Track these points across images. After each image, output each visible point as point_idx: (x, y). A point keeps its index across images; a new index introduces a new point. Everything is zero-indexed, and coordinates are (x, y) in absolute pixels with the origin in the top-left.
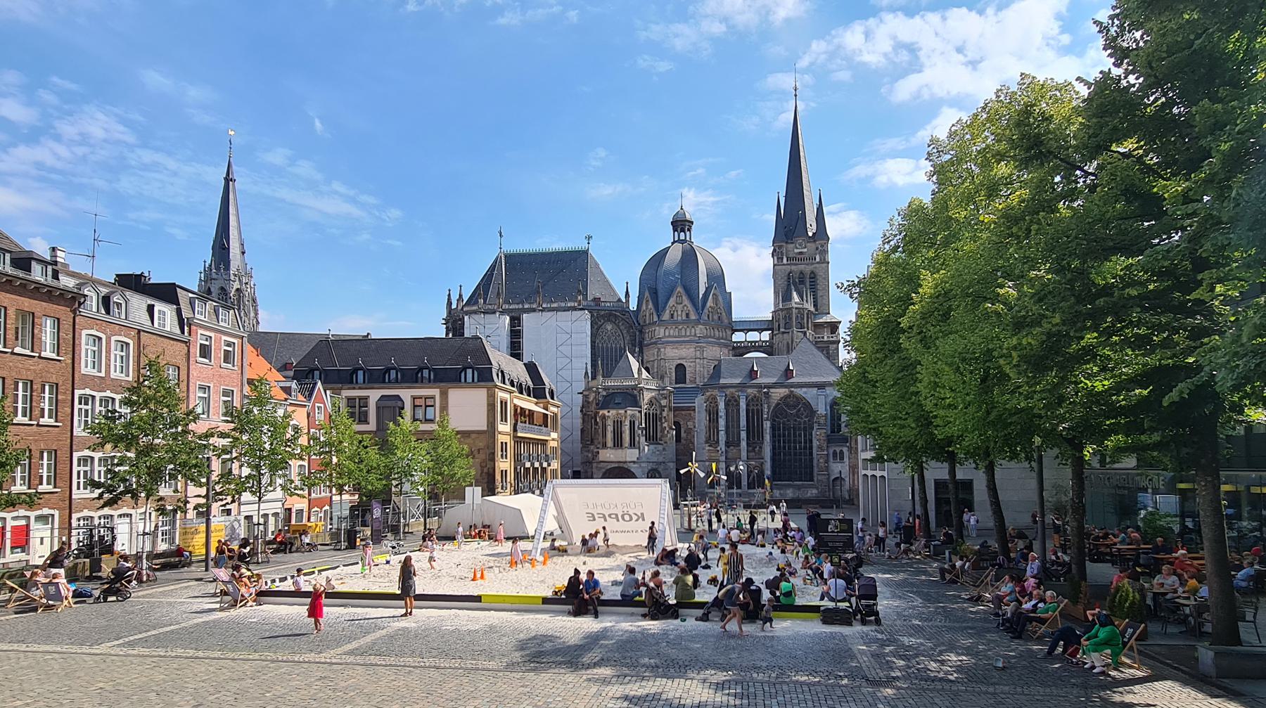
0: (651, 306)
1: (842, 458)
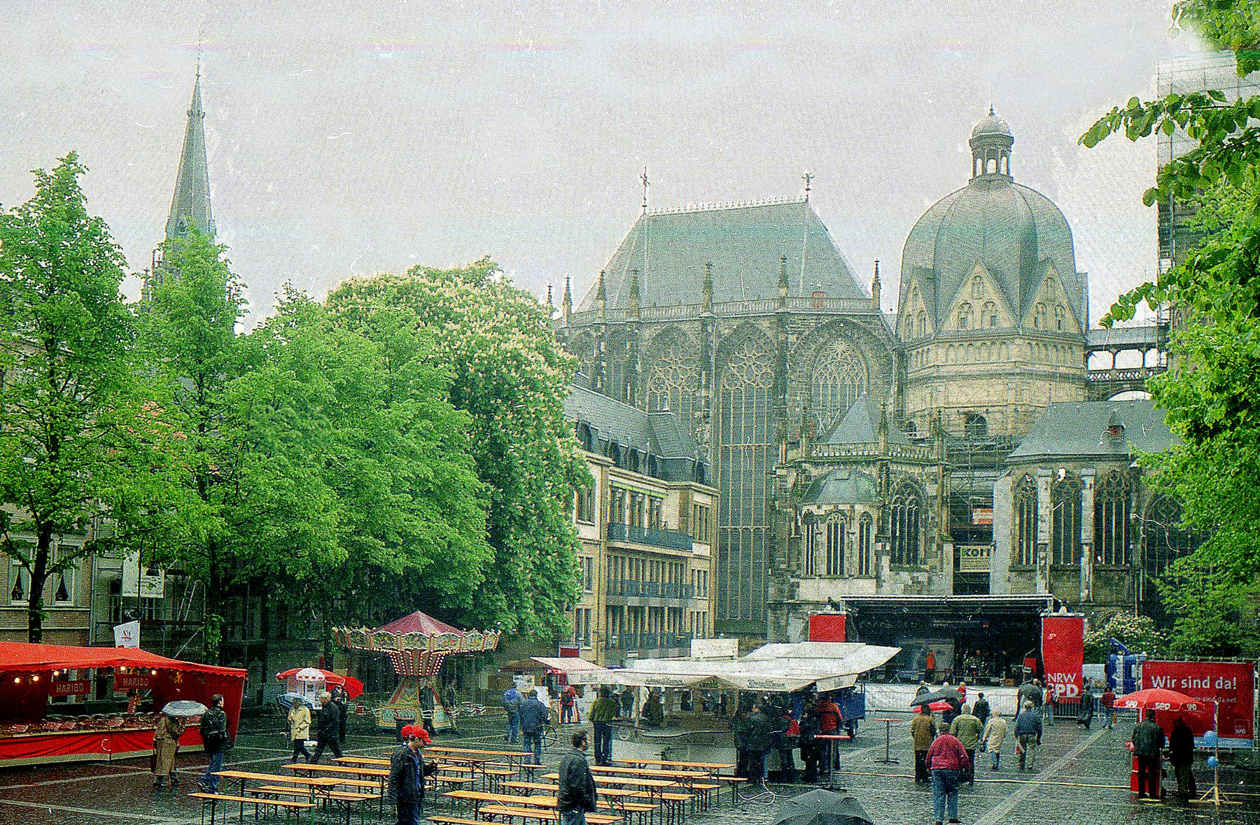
0: (921, 304)
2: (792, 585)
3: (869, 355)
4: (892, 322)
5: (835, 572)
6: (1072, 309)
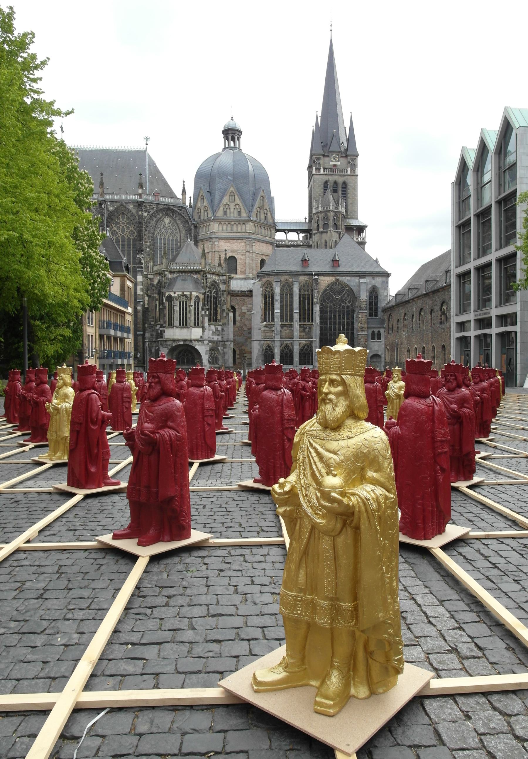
1: (379, 338)
2: (161, 331)
3: (181, 226)
4: (190, 210)
5: (183, 325)
6: (270, 212)
